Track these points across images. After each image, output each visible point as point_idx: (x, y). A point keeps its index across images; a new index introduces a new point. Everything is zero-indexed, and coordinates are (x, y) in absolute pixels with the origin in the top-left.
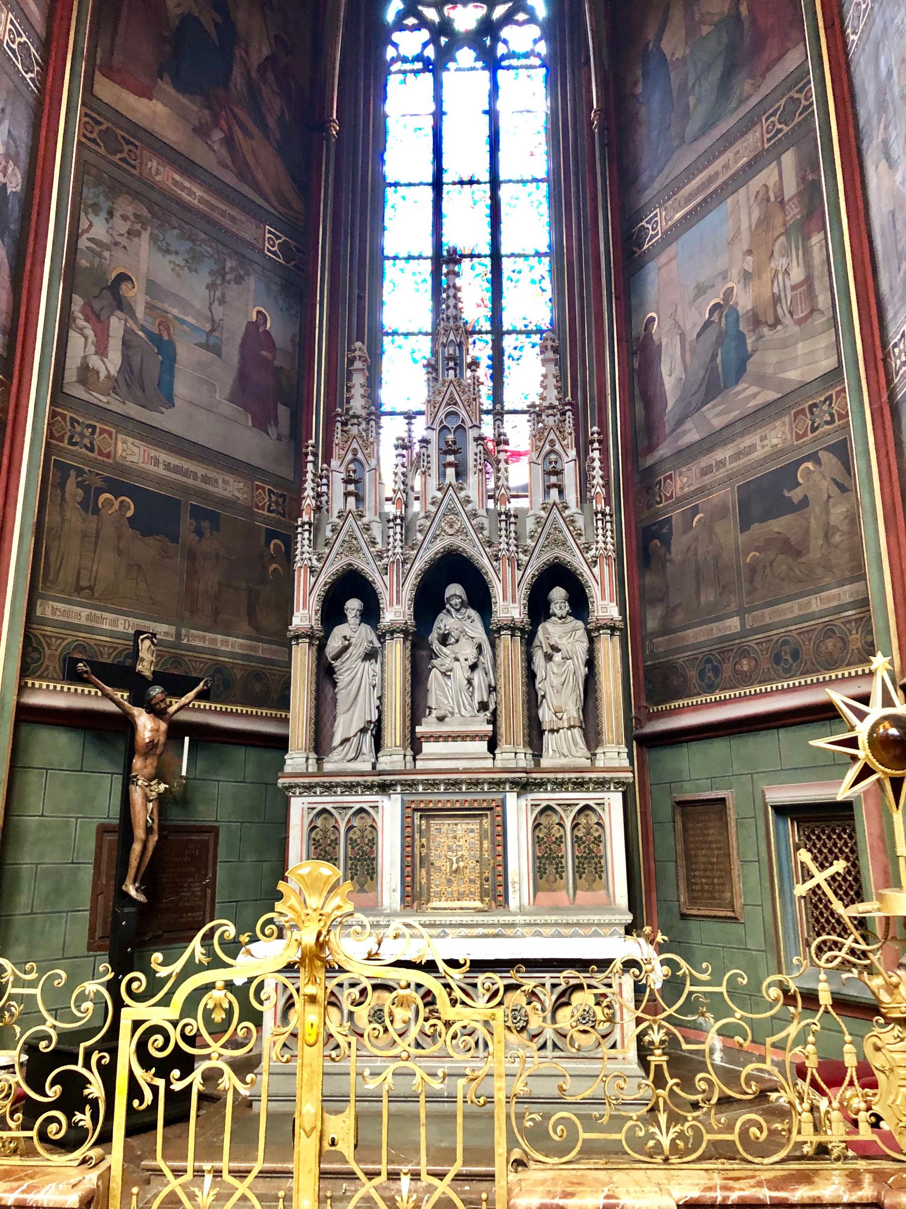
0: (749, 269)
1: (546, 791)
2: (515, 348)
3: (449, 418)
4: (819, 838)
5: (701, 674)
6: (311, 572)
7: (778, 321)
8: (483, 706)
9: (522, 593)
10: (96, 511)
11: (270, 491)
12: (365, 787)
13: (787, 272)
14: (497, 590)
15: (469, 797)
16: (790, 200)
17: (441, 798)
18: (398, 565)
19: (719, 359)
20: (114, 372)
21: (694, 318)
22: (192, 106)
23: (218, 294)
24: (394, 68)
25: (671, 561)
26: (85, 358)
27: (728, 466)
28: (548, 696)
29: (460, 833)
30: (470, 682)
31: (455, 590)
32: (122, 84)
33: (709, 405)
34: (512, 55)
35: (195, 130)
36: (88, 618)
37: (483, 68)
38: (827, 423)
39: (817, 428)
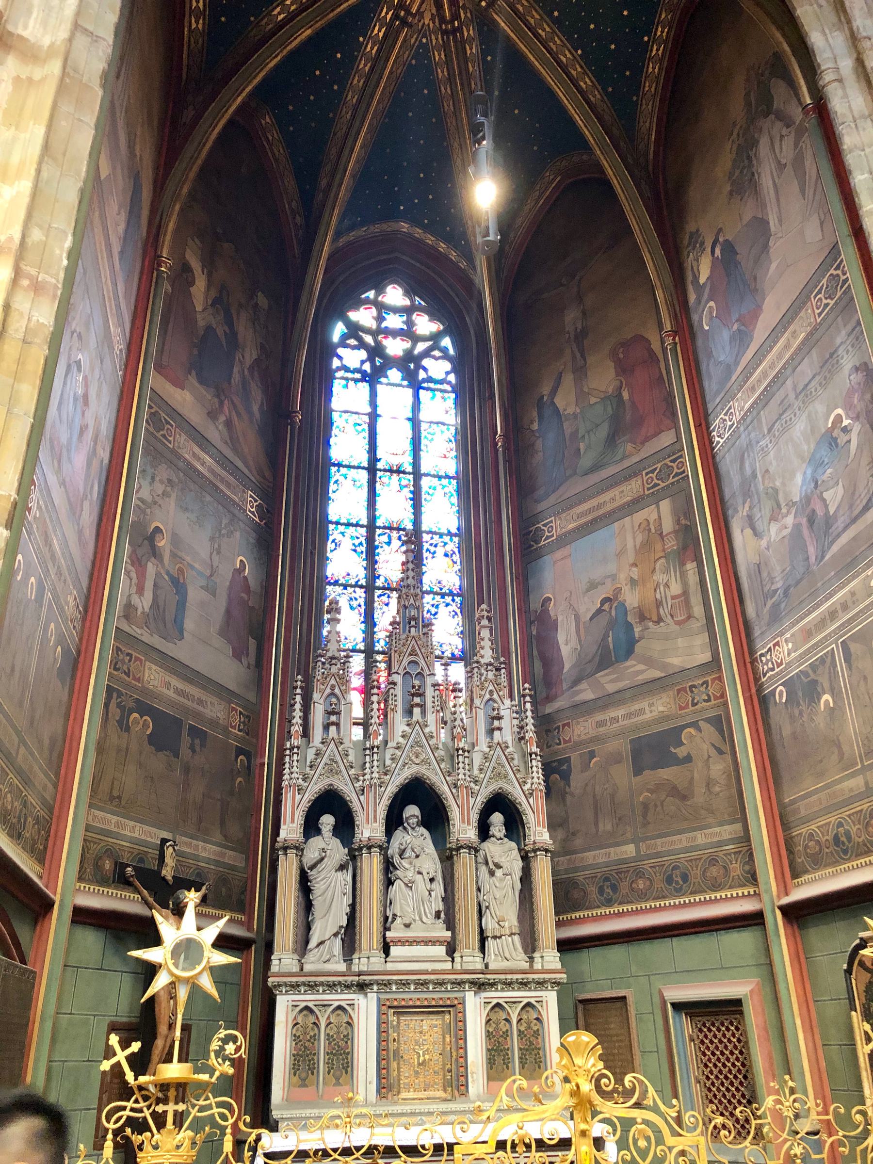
0: (636, 577)
1: (497, 990)
2: (433, 605)
3: (411, 665)
4: (710, 1030)
5: (601, 891)
7: (660, 620)
8: (438, 915)
9: (475, 817)
10: (128, 729)
11: (241, 713)
13: (667, 585)
14: (455, 814)
15: (436, 996)
16: (667, 535)
17: (412, 996)
18: (375, 788)
19: (610, 639)
20: (147, 609)
21: (588, 606)
22: (208, 395)
23: (216, 546)
24: (338, 374)
25: (572, 795)
26: (130, 595)
27: (621, 723)
28: (491, 907)
30: (430, 892)
32: (166, 377)
34: (430, 380)
35: (208, 414)
36: (117, 824)
37: (408, 386)
38: (705, 701)
39: (696, 704)
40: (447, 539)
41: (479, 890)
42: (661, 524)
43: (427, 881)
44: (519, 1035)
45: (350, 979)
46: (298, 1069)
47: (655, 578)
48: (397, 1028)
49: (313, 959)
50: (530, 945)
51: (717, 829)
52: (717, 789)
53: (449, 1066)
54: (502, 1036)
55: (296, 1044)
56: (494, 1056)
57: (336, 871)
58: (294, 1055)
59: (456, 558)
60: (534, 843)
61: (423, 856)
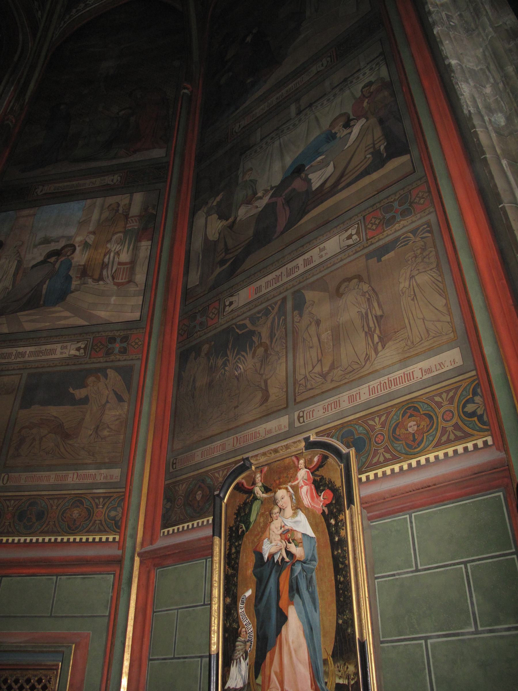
0: (91, 243)
7: (101, 278)
13: (118, 254)
16: (133, 217)
19: (45, 286)
33: (22, 313)
42: (129, 209)
47: (109, 246)
51: (93, 472)
52: (106, 433)
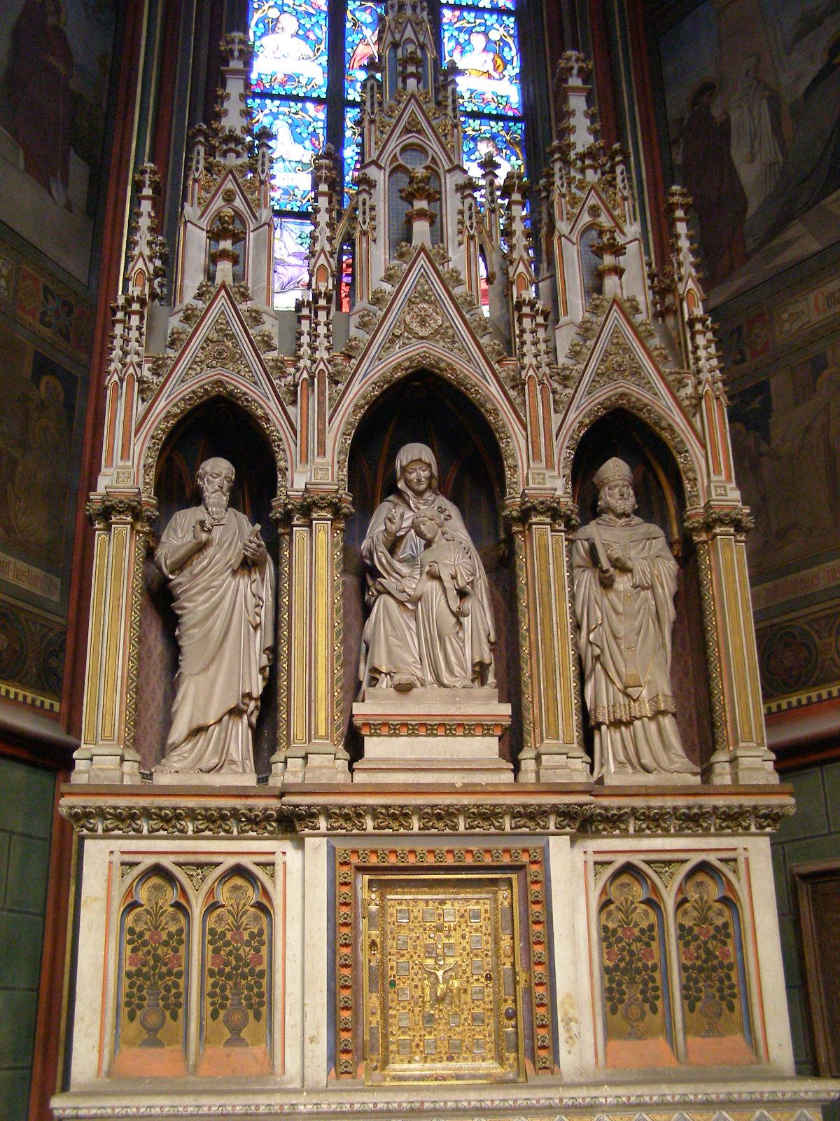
3: (408, 154)
6: (141, 391)
8: (480, 672)
9: (563, 452)
12: (249, 820)
14: (516, 442)
17: (413, 844)
29: (450, 920)
31: (416, 457)
40: (491, 19)
41: (577, 627)
43: (452, 594)
44: (680, 937)
45: (261, 803)
46: (140, 1007)
48: (377, 920)
49: (177, 766)
50: (703, 734)
53: (510, 1004)
54: (639, 939)
55: (134, 950)
56: (620, 983)
57: (234, 573)
58: (129, 975)
59: (511, 53)
60: (708, 506)
61: (440, 541)
